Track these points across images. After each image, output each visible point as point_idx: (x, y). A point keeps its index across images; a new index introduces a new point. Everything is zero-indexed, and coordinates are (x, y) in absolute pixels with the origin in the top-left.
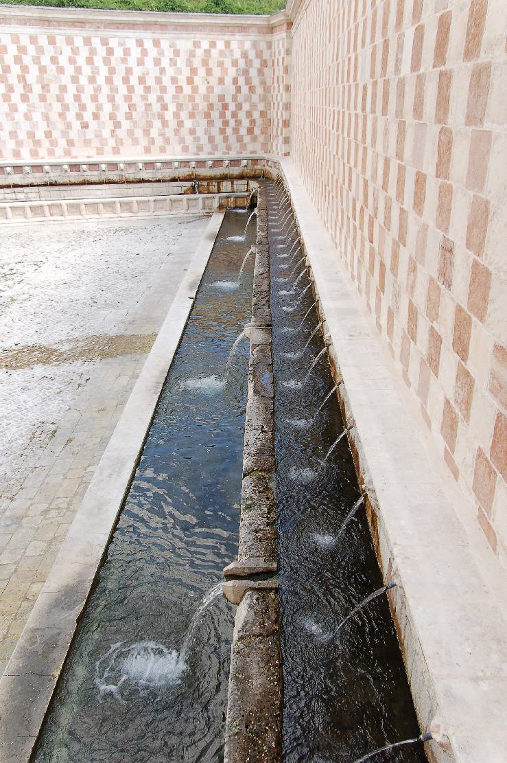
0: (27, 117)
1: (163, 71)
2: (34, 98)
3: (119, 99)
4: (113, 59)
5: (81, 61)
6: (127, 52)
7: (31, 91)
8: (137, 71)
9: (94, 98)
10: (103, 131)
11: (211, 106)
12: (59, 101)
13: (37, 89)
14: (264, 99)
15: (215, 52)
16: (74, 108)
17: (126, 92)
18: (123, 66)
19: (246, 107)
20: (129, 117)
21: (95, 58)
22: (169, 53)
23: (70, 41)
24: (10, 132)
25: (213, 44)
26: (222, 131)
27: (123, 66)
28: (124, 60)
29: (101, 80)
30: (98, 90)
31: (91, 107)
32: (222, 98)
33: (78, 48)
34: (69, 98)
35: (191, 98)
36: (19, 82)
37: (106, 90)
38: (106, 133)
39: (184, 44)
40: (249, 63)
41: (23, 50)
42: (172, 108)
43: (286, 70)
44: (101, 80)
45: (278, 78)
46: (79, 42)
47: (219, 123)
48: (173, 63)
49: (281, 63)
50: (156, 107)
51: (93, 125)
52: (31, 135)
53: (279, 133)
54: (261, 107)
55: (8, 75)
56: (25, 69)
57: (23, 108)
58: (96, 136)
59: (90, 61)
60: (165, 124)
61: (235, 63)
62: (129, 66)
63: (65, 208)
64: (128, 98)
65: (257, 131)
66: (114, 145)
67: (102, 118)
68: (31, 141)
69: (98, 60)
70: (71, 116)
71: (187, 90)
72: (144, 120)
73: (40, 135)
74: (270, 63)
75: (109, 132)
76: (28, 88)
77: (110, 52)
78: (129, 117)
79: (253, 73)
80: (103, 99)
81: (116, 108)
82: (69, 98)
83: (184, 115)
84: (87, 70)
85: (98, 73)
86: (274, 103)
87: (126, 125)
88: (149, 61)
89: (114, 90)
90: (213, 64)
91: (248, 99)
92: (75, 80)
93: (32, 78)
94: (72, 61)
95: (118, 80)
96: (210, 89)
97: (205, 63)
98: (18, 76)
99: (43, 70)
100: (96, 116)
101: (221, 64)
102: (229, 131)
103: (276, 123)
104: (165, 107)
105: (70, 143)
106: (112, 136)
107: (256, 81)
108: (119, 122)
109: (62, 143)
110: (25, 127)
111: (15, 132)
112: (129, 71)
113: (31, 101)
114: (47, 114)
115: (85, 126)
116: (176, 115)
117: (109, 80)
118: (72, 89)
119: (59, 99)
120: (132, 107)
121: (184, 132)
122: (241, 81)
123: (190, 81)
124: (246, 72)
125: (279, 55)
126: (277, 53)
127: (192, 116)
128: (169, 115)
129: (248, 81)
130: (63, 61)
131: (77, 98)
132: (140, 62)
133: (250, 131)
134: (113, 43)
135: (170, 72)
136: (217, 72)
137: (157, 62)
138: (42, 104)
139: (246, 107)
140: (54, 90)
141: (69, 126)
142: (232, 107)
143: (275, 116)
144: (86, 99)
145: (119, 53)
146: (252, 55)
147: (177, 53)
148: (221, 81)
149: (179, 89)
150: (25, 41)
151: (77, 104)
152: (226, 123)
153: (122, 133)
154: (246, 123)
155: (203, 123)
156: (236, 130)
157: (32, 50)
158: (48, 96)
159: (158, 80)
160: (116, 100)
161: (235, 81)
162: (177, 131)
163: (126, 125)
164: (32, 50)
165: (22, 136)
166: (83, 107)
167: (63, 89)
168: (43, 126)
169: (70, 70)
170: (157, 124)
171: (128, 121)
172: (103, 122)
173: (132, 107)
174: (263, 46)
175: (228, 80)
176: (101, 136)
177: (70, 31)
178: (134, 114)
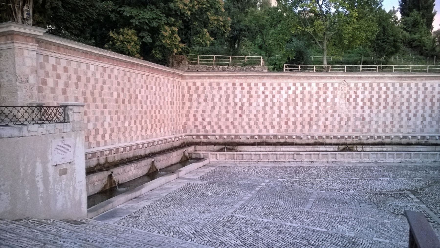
0: (384, 115)
2: (388, 108)
3: (427, 108)
4: (427, 92)
5: (412, 92)
7: (388, 105)
9: (416, 108)
10: (417, 121)
12: (399, 109)
13: (391, 104)
16: (406, 111)
17: (431, 105)
18: (431, 94)
20: (430, 116)
21: (419, 91)
24: (376, 122)
27: (431, 94)
28: (432, 92)
29: (420, 100)
30: (418, 104)
31: (413, 111)
33: (412, 87)
34: (404, 108)
36: (384, 101)
37: (421, 105)
38: (418, 123)
41: (388, 89)
44: (420, 100)
46: (413, 85)
51: (413, 119)
55: (380, 98)
56: (387, 96)
57: (383, 111)
58: (414, 124)
59: (416, 92)
62: (434, 94)
63: (412, 155)
64: (431, 108)
66: (422, 128)
67: (418, 116)
68: (383, 125)
69: (420, 92)
70: (403, 115)
72: (437, 117)
73: (388, 123)
75: (420, 122)
76: (387, 103)
78: (430, 116)
80: (419, 108)
81: (425, 111)
82: (404, 108)
84: (414, 96)
85: (419, 97)
87: (428, 119)
89: (425, 104)
92: (408, 100)
93: (389, 100)
94: (408, 93)
95: (427, 100)
98: (384, 99)
99: (395, 96)
105: (401, 126)
106: (421, 124)
108: (425, 118)
109: (397, 126)
110: (383, 119)
111: (378, 121)
112: (434, 96)
113: (387, 109)
114: (393, 114)
115: (409, 119)
117: (424, 100)
118: (406, 104)
119: (399, 108)
120: (433, 111)
130: (404, 93)
131: (408, 107)
134: (428, 85)
138: (392, 110)
140: (398, 104)
141: (402, 119)
144: (411, 108)
145: (430, 89)
150: (389, 85)
151: (407, 110)
153: (426, 123)
157: (392, 89)
158: (395, 106)
160: (426, 108)
164: (392, 89)
165: (380, 123)
166: (410, 111)
167: (402, 104)
168: (390, 119)
169: (407, 96)
171: (430, 117)
172: (418, 118)
176: (416, 124)
178: (433, 115)
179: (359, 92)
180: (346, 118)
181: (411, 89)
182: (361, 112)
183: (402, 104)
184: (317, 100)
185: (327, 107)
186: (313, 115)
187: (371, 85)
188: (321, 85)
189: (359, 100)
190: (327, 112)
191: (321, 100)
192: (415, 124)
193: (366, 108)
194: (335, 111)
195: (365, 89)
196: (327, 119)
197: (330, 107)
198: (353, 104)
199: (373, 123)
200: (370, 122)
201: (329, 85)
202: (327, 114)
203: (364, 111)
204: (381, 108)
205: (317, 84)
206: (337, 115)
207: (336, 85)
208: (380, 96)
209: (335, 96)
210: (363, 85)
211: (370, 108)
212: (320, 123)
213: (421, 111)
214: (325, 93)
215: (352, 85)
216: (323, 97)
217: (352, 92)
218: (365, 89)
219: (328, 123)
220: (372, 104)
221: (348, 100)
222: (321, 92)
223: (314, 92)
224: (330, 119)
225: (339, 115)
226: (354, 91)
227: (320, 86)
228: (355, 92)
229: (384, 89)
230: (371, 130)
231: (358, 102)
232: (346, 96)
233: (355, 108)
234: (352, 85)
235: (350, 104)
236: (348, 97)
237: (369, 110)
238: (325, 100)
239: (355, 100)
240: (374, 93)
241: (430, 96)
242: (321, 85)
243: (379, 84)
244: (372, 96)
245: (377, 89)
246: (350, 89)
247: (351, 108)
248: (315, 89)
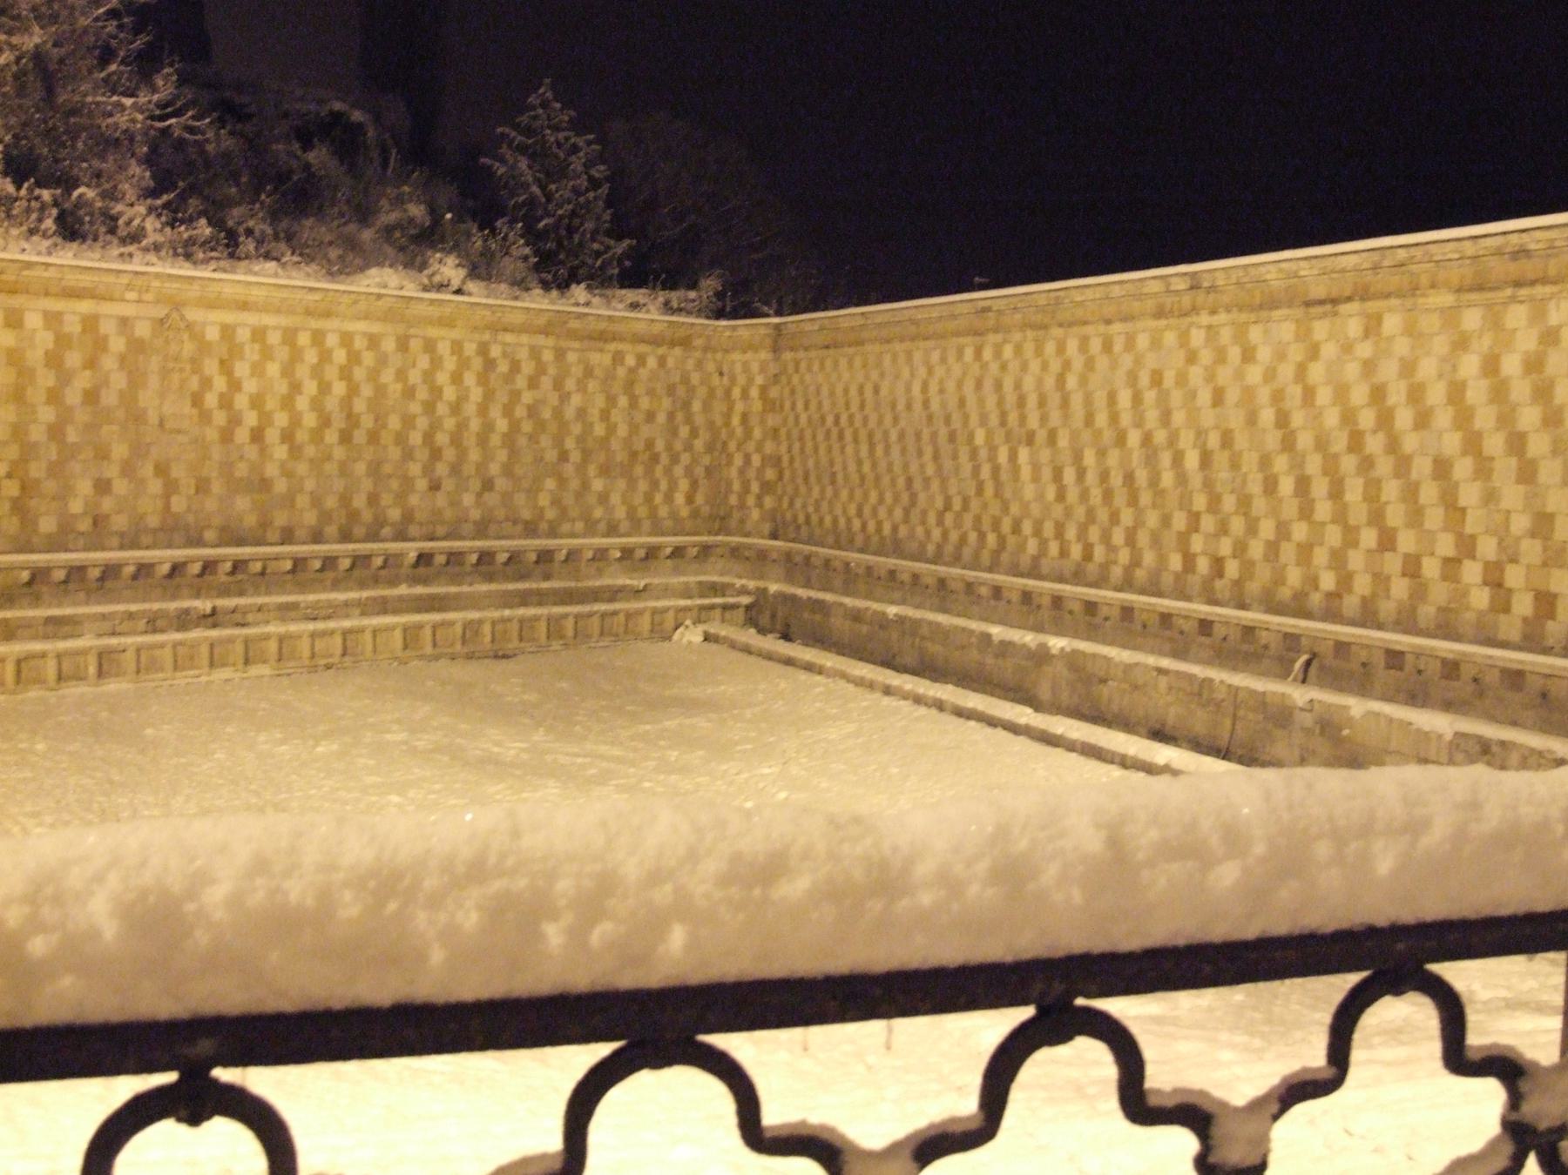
0: (344, 469)
1: (565, 397)
2: (360, 436)
4: (493, 376)
6: (515, 367)
8: (527, 397)
9: (456, 440)
11: (634, 455)
14: (710, 448)
15: (643, 373)
19: (685, 458)
20: (508, 471)
22: (577, 371)
23: (430, 346)
25: (641, 360)
26: (649, 498)
29: (470, 409)
31: (449, 454)
32: (650, 444)
35: (604, 442)
38: (468, 499)
39: (600, 359)
40: (691, 390)
42: (575, 456)
43: (770, 406)
44: (470, 409)
45: (745, 418)
47: (643, 486)
48: (582, 387)
49: (754, 393)
50: (551, 455)
51: (448, 485)
52: (345, 500)
53: (751, 500)
54: (706, 460)
56: (353, 391)
57: (339, 453)
59: (457, 378)
60: (562, 482)
61: (671, 390)
65: (700, 499)
69: (470, 379)
71: (599, 430)
73: (359, 502)
74: (719, 393)
77: (490, 364)
79: (696, 406)
80: (470, 440)
82: (416, 438)
83: (592, 470)
86: (730, 457)
88: (546, 383)
89: (488, 427)
90: (639, 389)
91: (689, 447)
92: (429, 407)
95: (495, 412)
96: (634, 429)
97: (629, 385)
100: (455, 470)
101: (651, 392)
102: (658, 498)
103: (736, 486)
104: (564, 457)
107: (699, 420)
112: (515, 395)
115: (435, 487)
116: (581, 468)
117: (483, 410)
118: (422, 423)
120: (514, 453)
121: (592, 499)
122: (680, 416)
123: (605, 415)
124: (686, 405)
125: (751, 380)
126: (741, 380)
127: (605, 471)
128: (569, 469)
129: (689, 420)
132: (533, 383)
133: (690, 499)
134: (495, 351)
135: (576, 400)
136: (645, 403)
137: (558, 385)
139: (685, 458)
140: (394, 423)
142: (665, 459)
143: (734, 472)
145: (503, 367)
146: (695, 378)
147: (589, 372)
148: (650, 417)
149: (589, 427)
150: (359, 343)
152: (655, 484)
154: (684, 485)
155: (621, 484)
156: (669, 498)
157: (368, 358)
159: (558, 413)
161: (671, 416)
162: (579, 495)
163: (501, 484)
169: (422, 394)
170: (550, 484)
173: (514, 453)
174: (711, 367)
175: (661, 418)
177: (433, 332)
179: (242, 369)
180: (193, 482)
181: (436, 363)
182: (252, 452)
183: (408, 421)
184: (54, 397)
185: (105, 429)
186: (36, 470)
187: (290, 336)
188: (73, 326)
189: (241, 402)
190: (103, 455)
191: (73, 396)
192: (455, 503)
193: (272, 435)
194: (139, 450)
195: (267, 354)
196: (102, 486)
197: (115, 428)
198: (220, 418)
199: (302, 501)
200: (289, 500)
201: (108, 327)
202: (105, 463)
203: (263, 451)
204: (331, 437)
205: (52, 319)
206: (151, 468)
207: (143, 330)
208: (325, 388)
209: (136, 380)
210: (259, 334)
211: (287, 437)
212: (76, 506)
213: (474, 455)
214: (91, 363)
215: (212, 334)
216: (83, 381)
217: (211, 367)
218: (267, 354)
219: (107, 504)
220: (296, 421)
221: (197, 400)
222: (73, 359)
223: (35, 357)
224: (121, 486)
225: (161, 470)
226: (222, 362)
227: (67, 329)
228: (226, 367)
229: (340, 356)
230: (297, 533)
231: (240, 411)
232: (183, 382)
233: (227, 436)
234: (212, 334)
235: (205, 417)
236: (194, 383)
237: (285, 447)
238: (91, 397)
239: (226, 402)
240: (302, 372)
241: (502, 397)
242: (73, 326)
243: (318, 337)
244: (296, 388)
245: (311, 356)
246: (204, 347)
247: (212, 434)
248: (45, 340)
